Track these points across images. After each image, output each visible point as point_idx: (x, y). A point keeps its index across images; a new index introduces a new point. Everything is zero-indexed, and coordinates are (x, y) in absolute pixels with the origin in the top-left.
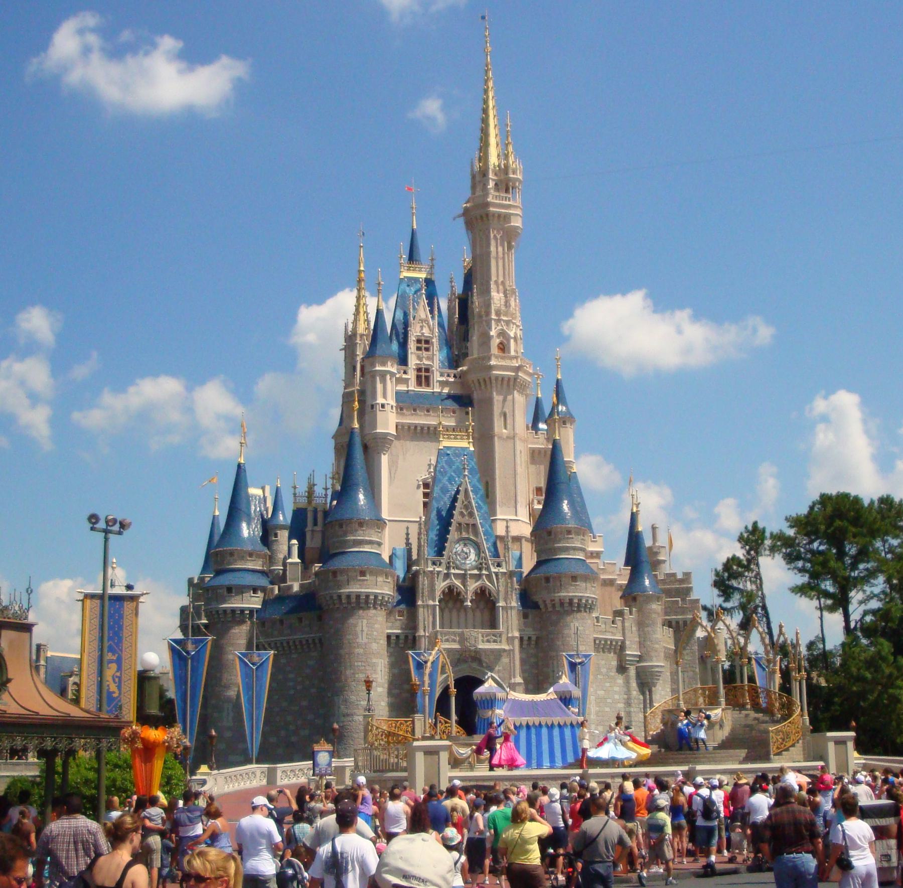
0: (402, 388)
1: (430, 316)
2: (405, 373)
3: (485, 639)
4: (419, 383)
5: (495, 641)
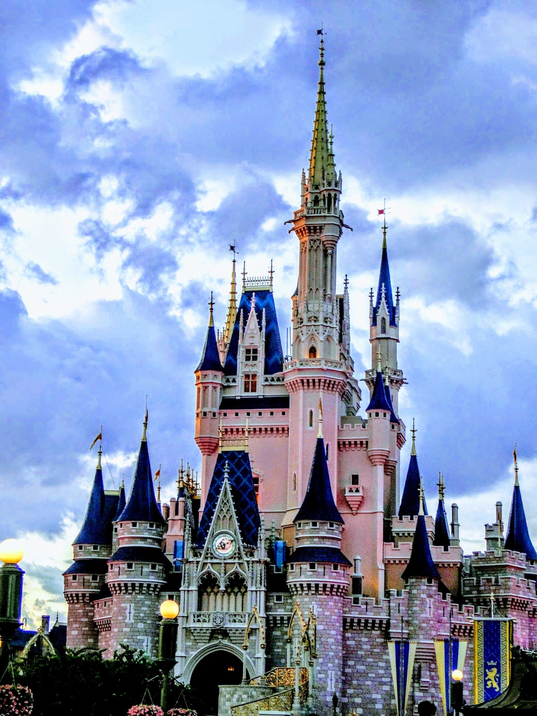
0: (231, 394)
1: (258, 327)
3: (231, 620)
4: (246, 390)
5: (241, 621)
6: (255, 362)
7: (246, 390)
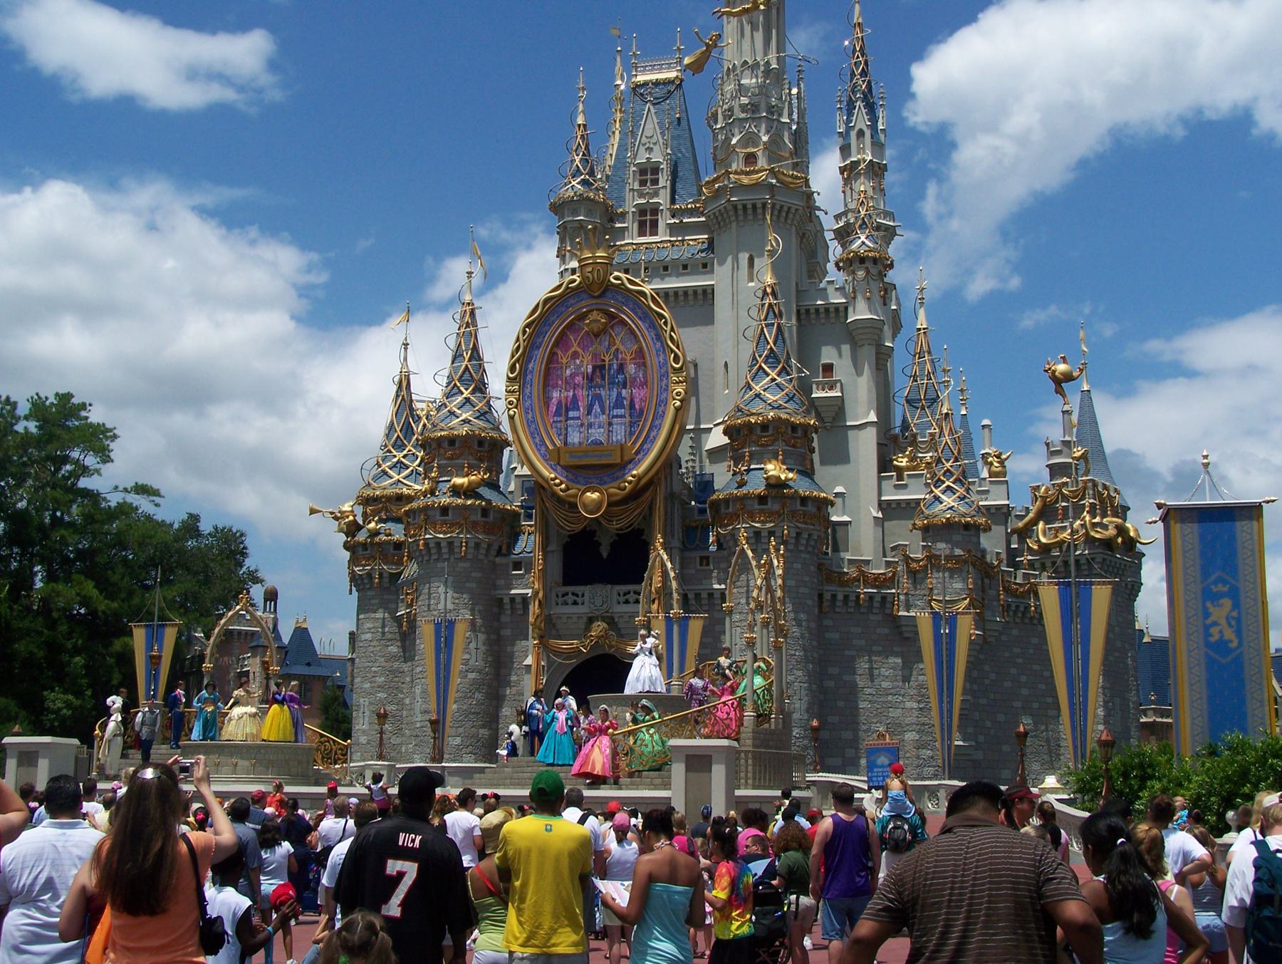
3: (622, 599)
7: (642, 233)
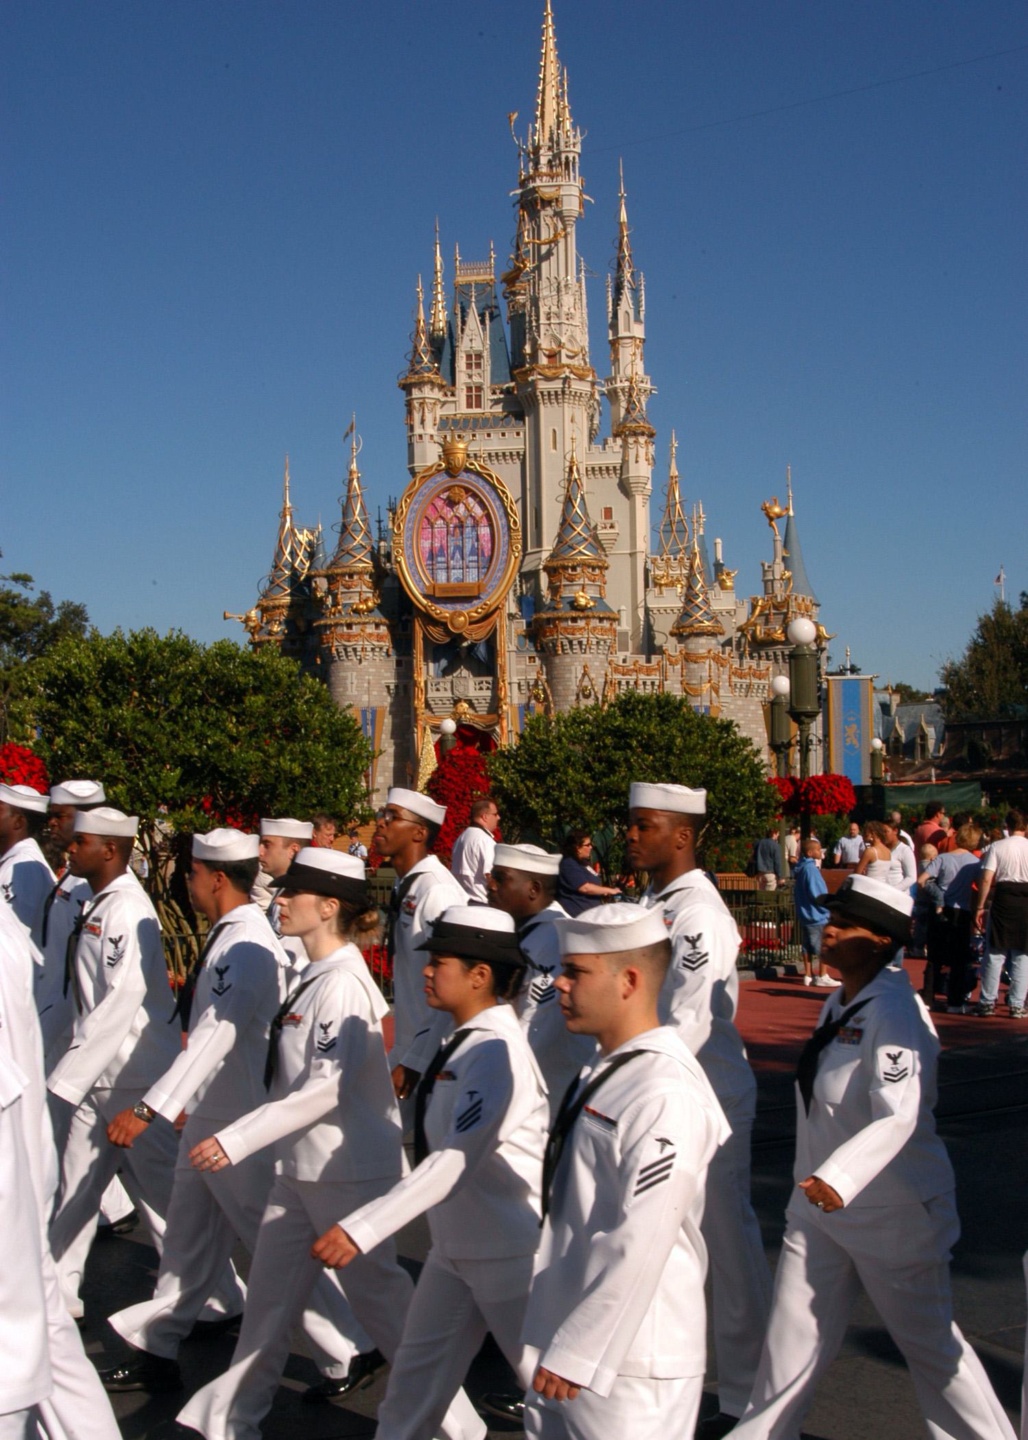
0: (449, 411)
2: (453, 395)
3: (478, 687)
4: (469, 405)
6: (479, 371)
